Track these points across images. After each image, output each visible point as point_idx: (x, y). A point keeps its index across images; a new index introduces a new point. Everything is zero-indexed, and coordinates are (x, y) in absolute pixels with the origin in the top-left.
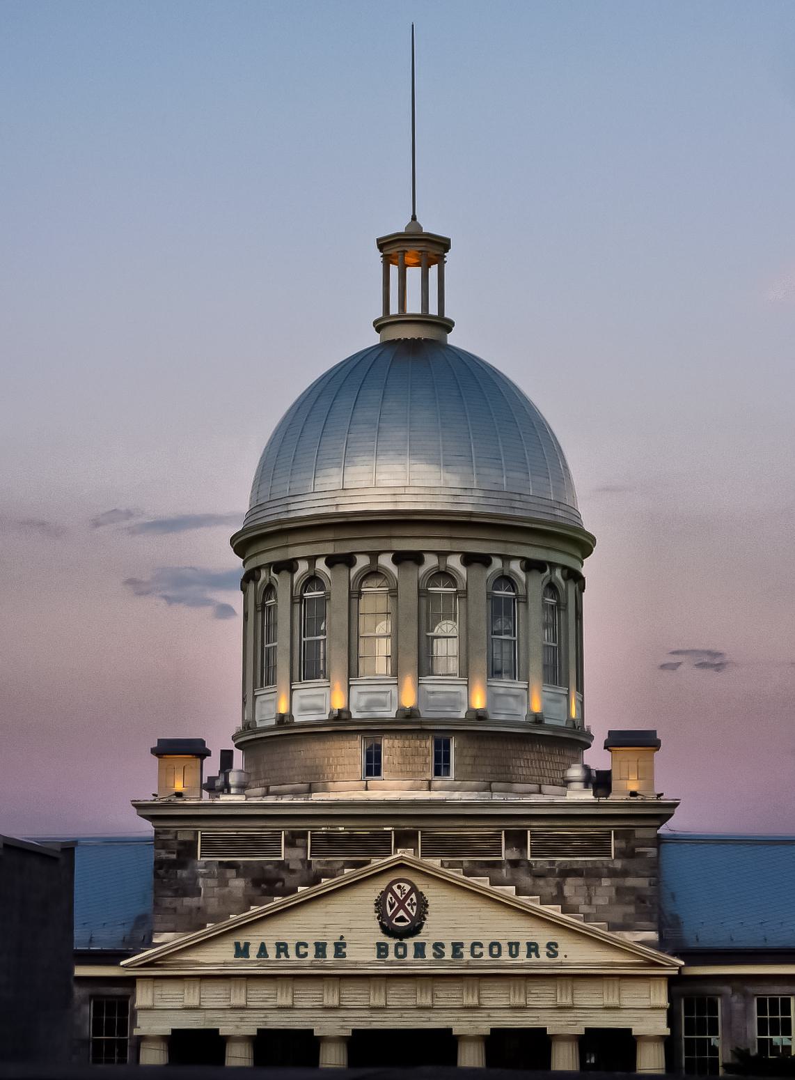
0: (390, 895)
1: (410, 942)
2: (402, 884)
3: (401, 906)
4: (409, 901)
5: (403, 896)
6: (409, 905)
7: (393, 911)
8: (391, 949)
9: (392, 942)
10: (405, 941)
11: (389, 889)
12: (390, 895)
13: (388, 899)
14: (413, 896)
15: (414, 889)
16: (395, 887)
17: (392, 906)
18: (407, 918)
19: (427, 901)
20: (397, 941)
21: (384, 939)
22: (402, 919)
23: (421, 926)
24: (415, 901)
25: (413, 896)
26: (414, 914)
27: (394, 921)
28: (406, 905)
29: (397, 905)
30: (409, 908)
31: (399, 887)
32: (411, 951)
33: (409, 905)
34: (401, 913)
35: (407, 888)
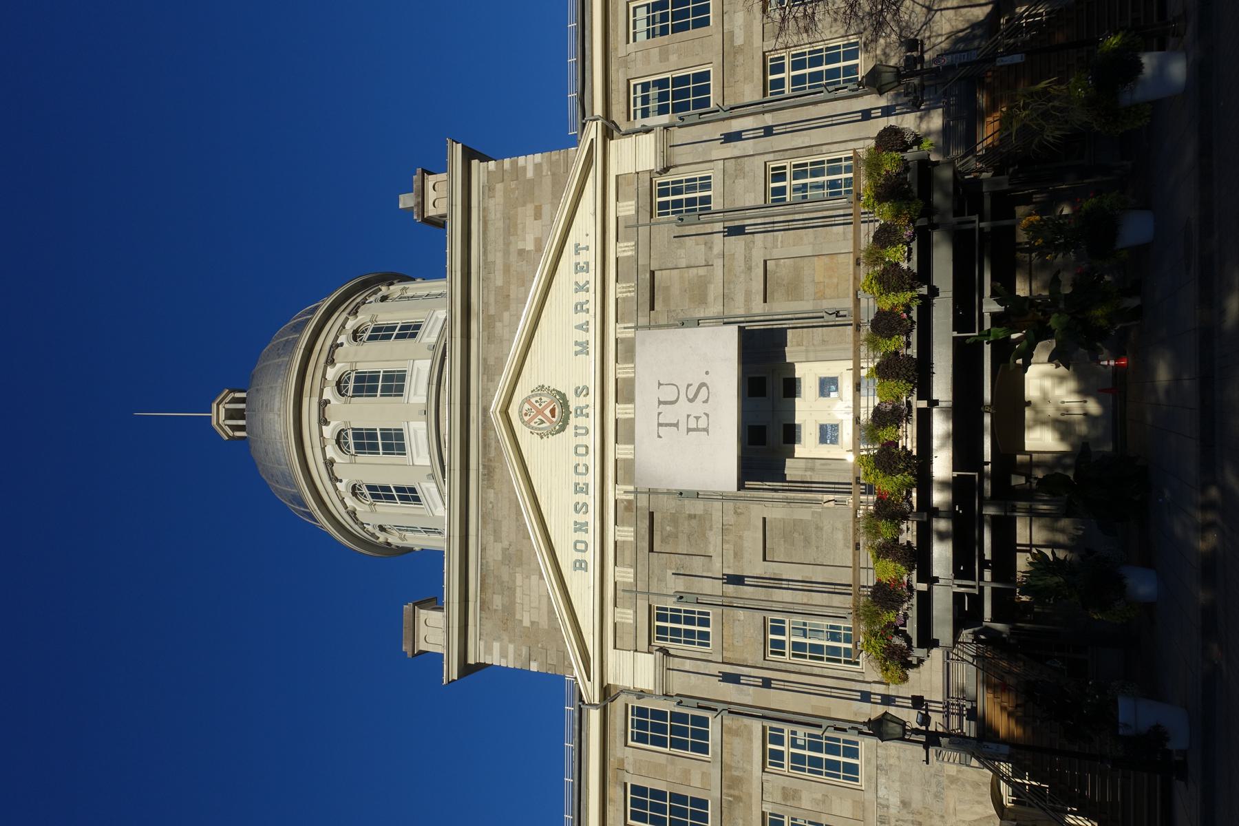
0: (532, 424)
1: (573, 403)
2: (524, 412)
3: (540, 412)
4: (537, 405)
5: (533, 410)
6: (540, 405)
7: (546, 421)
8: (581, 421)
9: (573, 420)
10: (572, 409)
11: (527, 424)
12: (532, 424)
13: (536, 425)
14: (533, 400)
15: (527, 400)
16: (527, 418)
17: (542, 422)
18: (552, 407)
19: (539, 386)
20: (572, 416)
21: (570, 429)
22: (553, 412)
23: (559, 393)
24: (538, 398)
25: (533, 400)
26: (548, 400)
27: (554, 420)
28: (540, 408)
29: (540, 417)
30: (543, 404)
31: (526, 415)
32: (582, 401)
33: (540, 405)
34: (547, 412)
35: (527, 406)
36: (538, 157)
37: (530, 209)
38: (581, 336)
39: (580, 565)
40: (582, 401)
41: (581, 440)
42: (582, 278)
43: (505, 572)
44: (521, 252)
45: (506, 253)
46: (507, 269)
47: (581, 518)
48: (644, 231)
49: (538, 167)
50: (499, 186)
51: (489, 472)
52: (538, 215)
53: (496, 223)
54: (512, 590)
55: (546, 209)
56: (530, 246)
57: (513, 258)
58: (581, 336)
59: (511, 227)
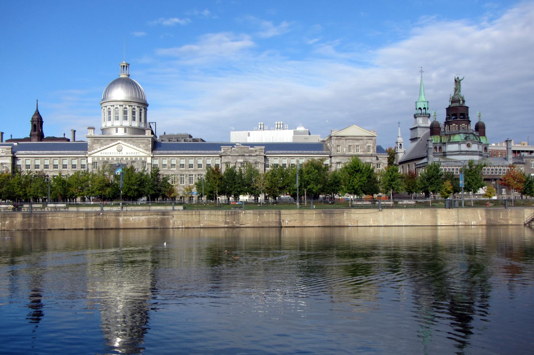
1: (121, 152)
21: (118, 152)
32: (121, 153)
36: (151, 147)
37: (145, 146)
38: (129, 153)
39: (101, 153)
40: (121, 153)
41: (116, 154)
42: (135, 153)
43: (100, 142)
44: (139, 145)
45: (140, 142)
46: (138, 142)
47: (107, 153)
48: (141, 161)
49: (150, 147)
50: (148, 141)
51: (112, 140)
52: (144, 147)
53: (143, 141)
54: (97, 143)
55: (144, 148)
56: (140, 146)
57: (139, 143)
58: (129, 153)
59: (143, 143)
